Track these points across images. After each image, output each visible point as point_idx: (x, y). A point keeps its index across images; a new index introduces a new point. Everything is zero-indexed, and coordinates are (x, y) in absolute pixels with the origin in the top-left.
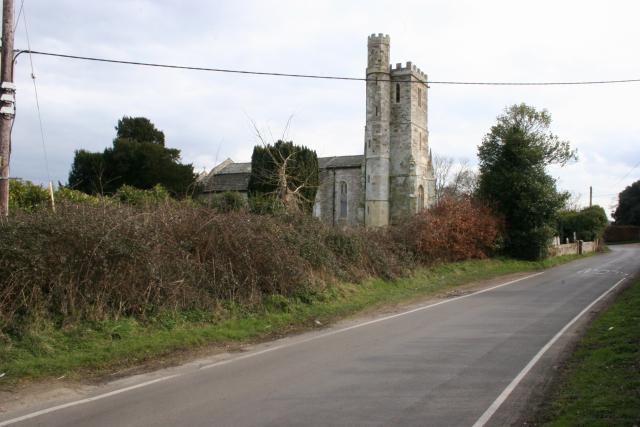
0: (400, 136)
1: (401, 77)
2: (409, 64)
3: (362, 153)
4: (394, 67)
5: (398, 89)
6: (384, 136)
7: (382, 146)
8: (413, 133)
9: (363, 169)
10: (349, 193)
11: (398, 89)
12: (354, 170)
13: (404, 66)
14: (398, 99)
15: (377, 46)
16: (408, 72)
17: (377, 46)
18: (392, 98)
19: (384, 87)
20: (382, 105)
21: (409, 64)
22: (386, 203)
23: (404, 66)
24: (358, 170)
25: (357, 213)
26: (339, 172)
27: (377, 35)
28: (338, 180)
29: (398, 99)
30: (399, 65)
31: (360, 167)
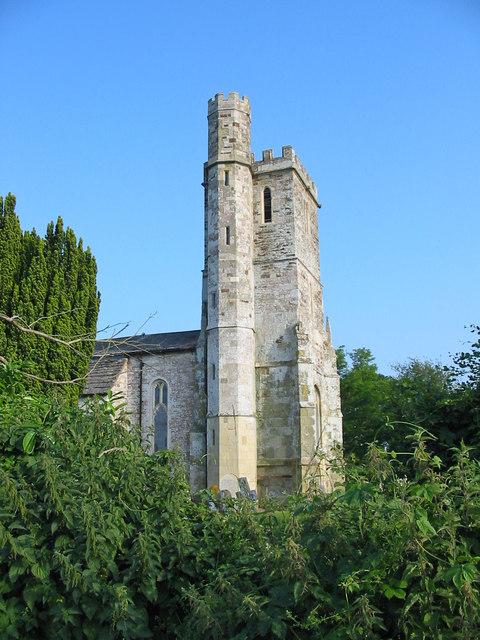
1: (270, 174)
2: (286, 150)
6: (244, 283)
7: (238, 303)
8: (300, 280)
9: (200, 352)
10: (171, 403)
12: (180, 357)
13: (276, 153)
14: (268, 217)
18: (255, 213)
20: (238, 224)
22: (253, 420)
23: (276, 153)
25: (188, 443)
26: (150, 361)
31: (193, 350)
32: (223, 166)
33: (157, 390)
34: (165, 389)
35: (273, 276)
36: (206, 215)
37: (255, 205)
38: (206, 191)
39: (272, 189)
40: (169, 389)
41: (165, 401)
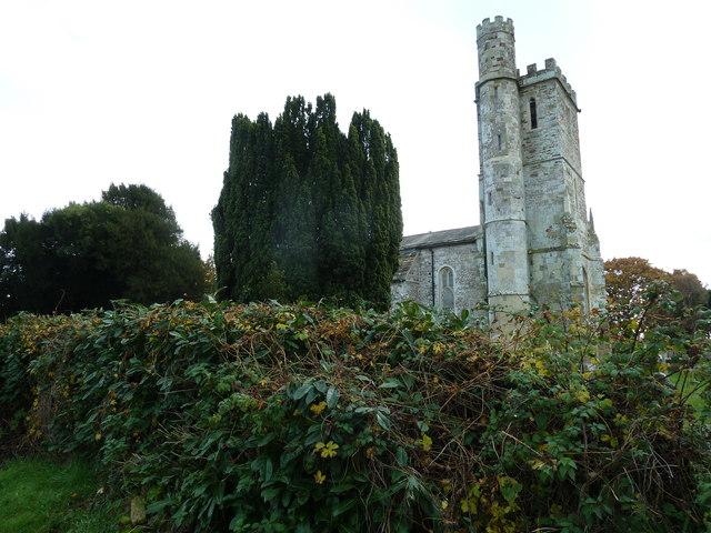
0: (542, 183)
1: (534, 85)
2: (550, 62)
3: (477, 222)
4: (523, 72)
5: (533, 106)
6: (514, 183)
7: (512, 199)
8: (566, 177)
9: (480, 244)
10: (456, 286)
11: (533, 106)
12: (463, 248)
13: (541, 66)
15: (495, 37)
16: (551, 74)
17: (495, 37)
18: (522, 122)
19: (508, 96)
21: (550, 62)
23: (541, 66)
24: (470, 246)
26: (438, 252)
27: (492, 20)
28: (438, 266)
29: (534, 124)
30: (532, 69)
31: (473, 241)
32: (492, 82)
33: (444, 276)
34: (451, 275)
35: (541, 174)
36: (480, 129)
37: (522, 114)
38: (478, 107)
39: (537, 99)
40: (454, 274)
41: (452, 285)
